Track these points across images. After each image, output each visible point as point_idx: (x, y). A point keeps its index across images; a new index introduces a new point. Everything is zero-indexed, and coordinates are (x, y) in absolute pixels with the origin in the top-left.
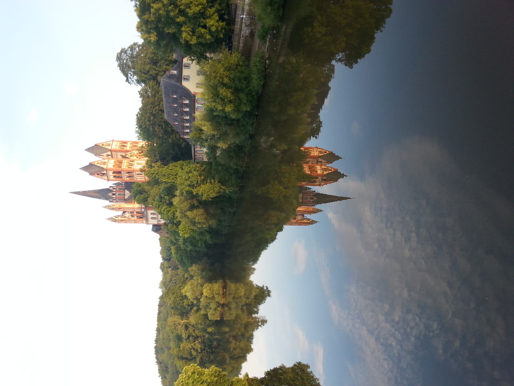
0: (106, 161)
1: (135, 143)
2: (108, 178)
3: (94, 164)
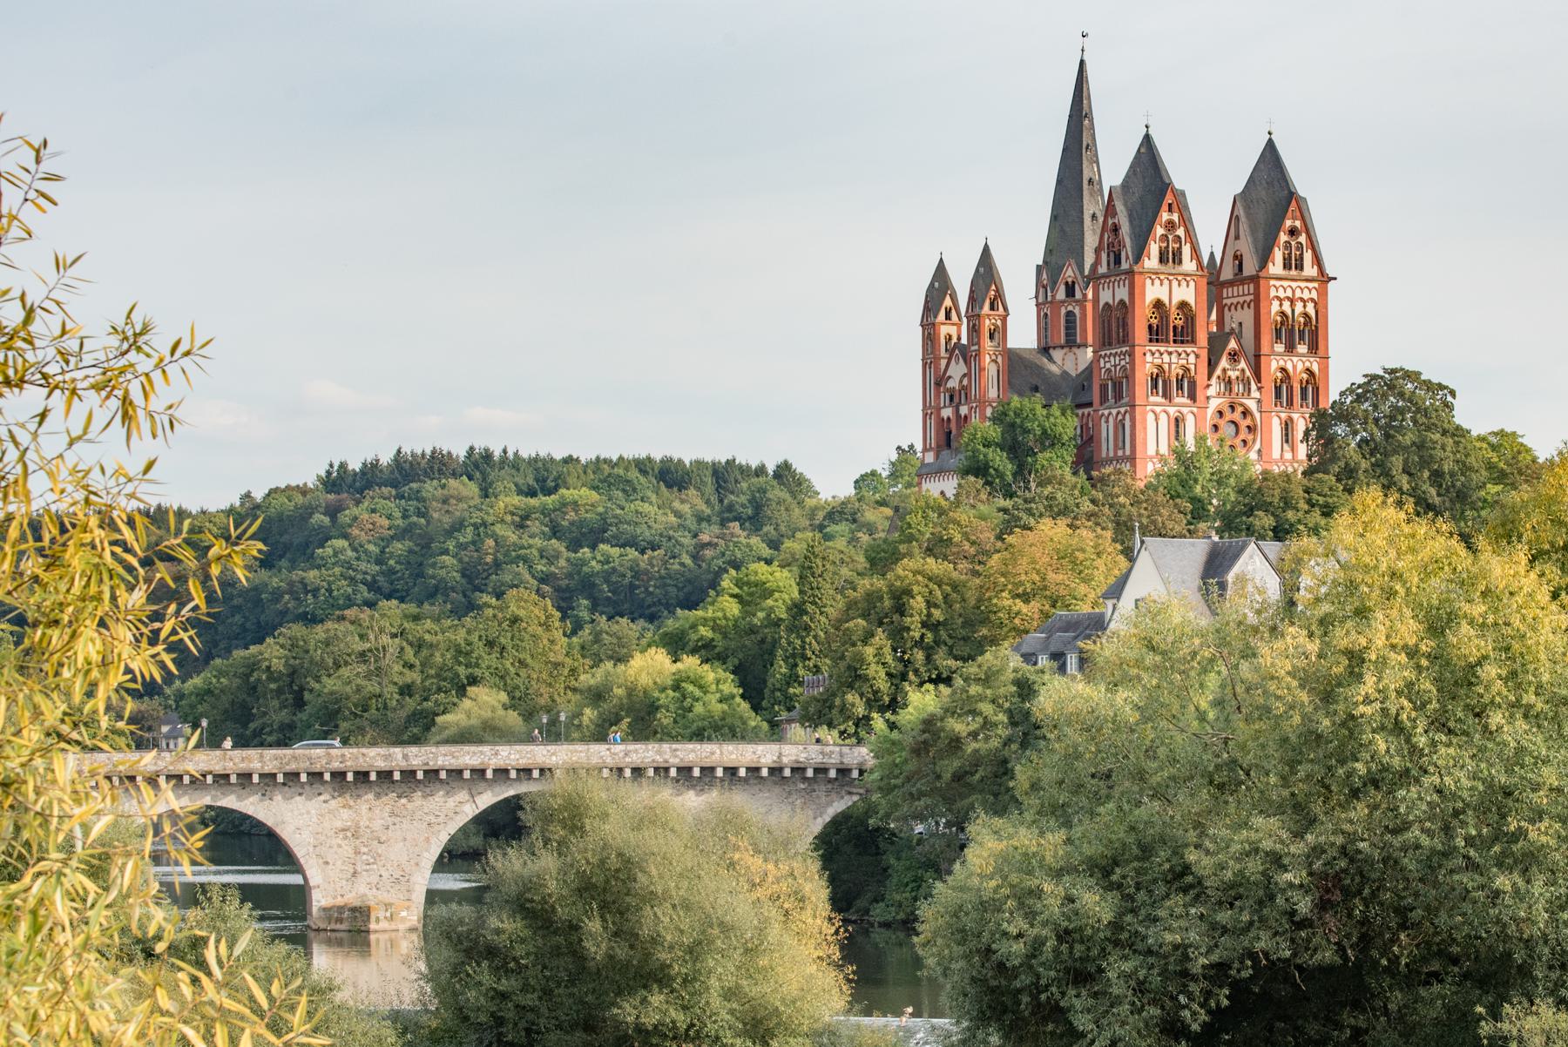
0: (1189, 265)
1: (1316, 390)
2: (1104, 276)
3: (1165, 207)
